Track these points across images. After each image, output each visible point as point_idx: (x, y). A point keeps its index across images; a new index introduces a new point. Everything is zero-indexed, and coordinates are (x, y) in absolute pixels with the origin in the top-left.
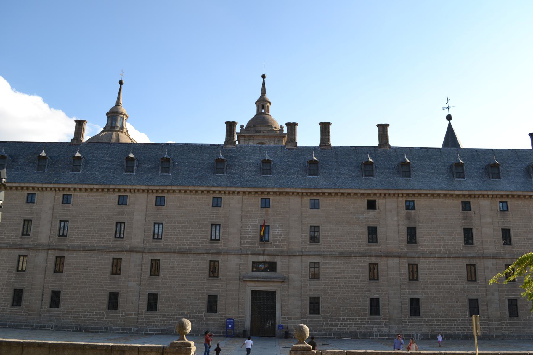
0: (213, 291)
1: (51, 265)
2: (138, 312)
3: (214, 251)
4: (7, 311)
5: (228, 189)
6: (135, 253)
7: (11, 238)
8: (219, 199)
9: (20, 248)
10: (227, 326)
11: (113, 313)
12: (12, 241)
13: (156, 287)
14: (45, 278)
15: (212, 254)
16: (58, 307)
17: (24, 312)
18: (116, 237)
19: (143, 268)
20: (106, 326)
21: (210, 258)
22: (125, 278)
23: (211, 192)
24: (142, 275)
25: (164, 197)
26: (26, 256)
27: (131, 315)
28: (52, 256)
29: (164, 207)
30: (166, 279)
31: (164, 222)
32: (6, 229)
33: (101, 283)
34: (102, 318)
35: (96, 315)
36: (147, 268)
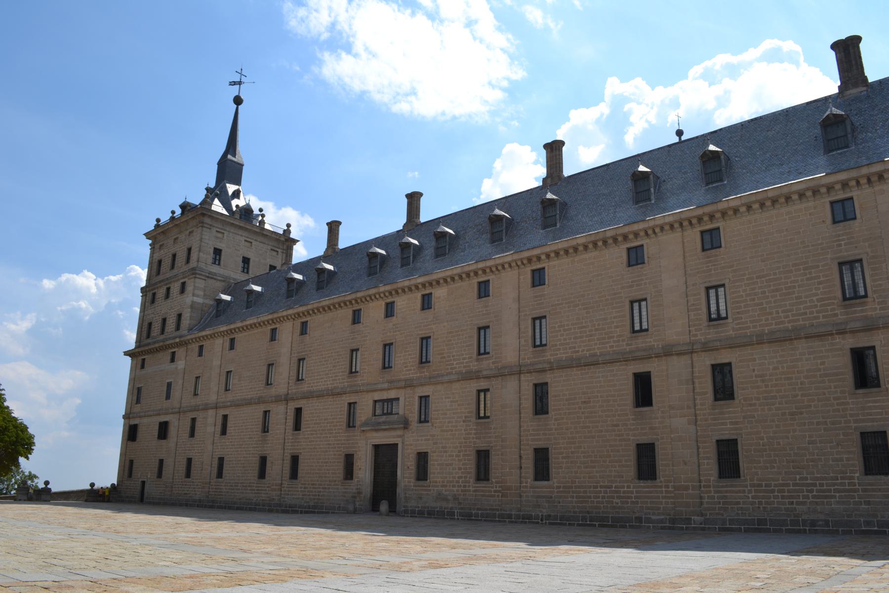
0: (873, 420)
1: (528, 403)
2: (700, 481)
3: (858, 325)
4: (469, 491)
5: (865, 171)
6: (675, 358)
7: (462, 363)
8: (848, 204)
9: (478, 378)
11: (648, 487)
12: (464, 367)
13: (731, 423)
15: (853, 332)
16: (548, 480)
17: (495, 491)
18: (634, 331)
19: (697, 385)
20: (637, 515)
22: (663, 412)
23: (823, 190)
24: (698, 402)
25: (718, 228)
26: (488, 390)
27: (686, 488)
29: (721, 249)
30: (751, 405)
31: (726, 282)
33: (617, 425)
34: (629, 497)
35: (617, 492)
36: (706, 385)
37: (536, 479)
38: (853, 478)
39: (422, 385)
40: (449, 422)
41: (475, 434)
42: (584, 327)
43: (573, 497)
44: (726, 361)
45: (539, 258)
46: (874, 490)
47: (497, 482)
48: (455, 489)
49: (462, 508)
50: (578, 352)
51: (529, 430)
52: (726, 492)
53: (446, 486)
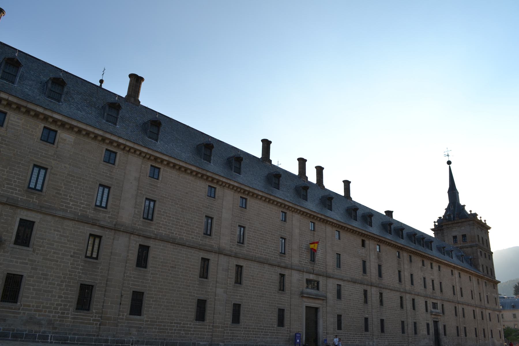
0: (282, 304)
1: (133, 257)
4: (68, 317)
6: (223, 256)
9: (94, 224)
10: (296, 340)
12: (80, 210)
14: (125, 273)
17: (94, 320)
21: (280, 271)
26: (100, 237)
28: (135, 243)
32: (72, 190)
33: (189, 286)
37: (131, 314)
38: (274, 327)
39: (28, 209)
40: (54, 253)
41: (81, 269)
42: (178, 219)
43: (156, 328)
44: (241, 265)
45: (162, 161)
46: (236, 330)
47: (96, 313)
48: (51, 315)
49: (56, 333)
50: (173, 233)
51: (131, 277)
52: (234, 330)
53: (41, 311)
